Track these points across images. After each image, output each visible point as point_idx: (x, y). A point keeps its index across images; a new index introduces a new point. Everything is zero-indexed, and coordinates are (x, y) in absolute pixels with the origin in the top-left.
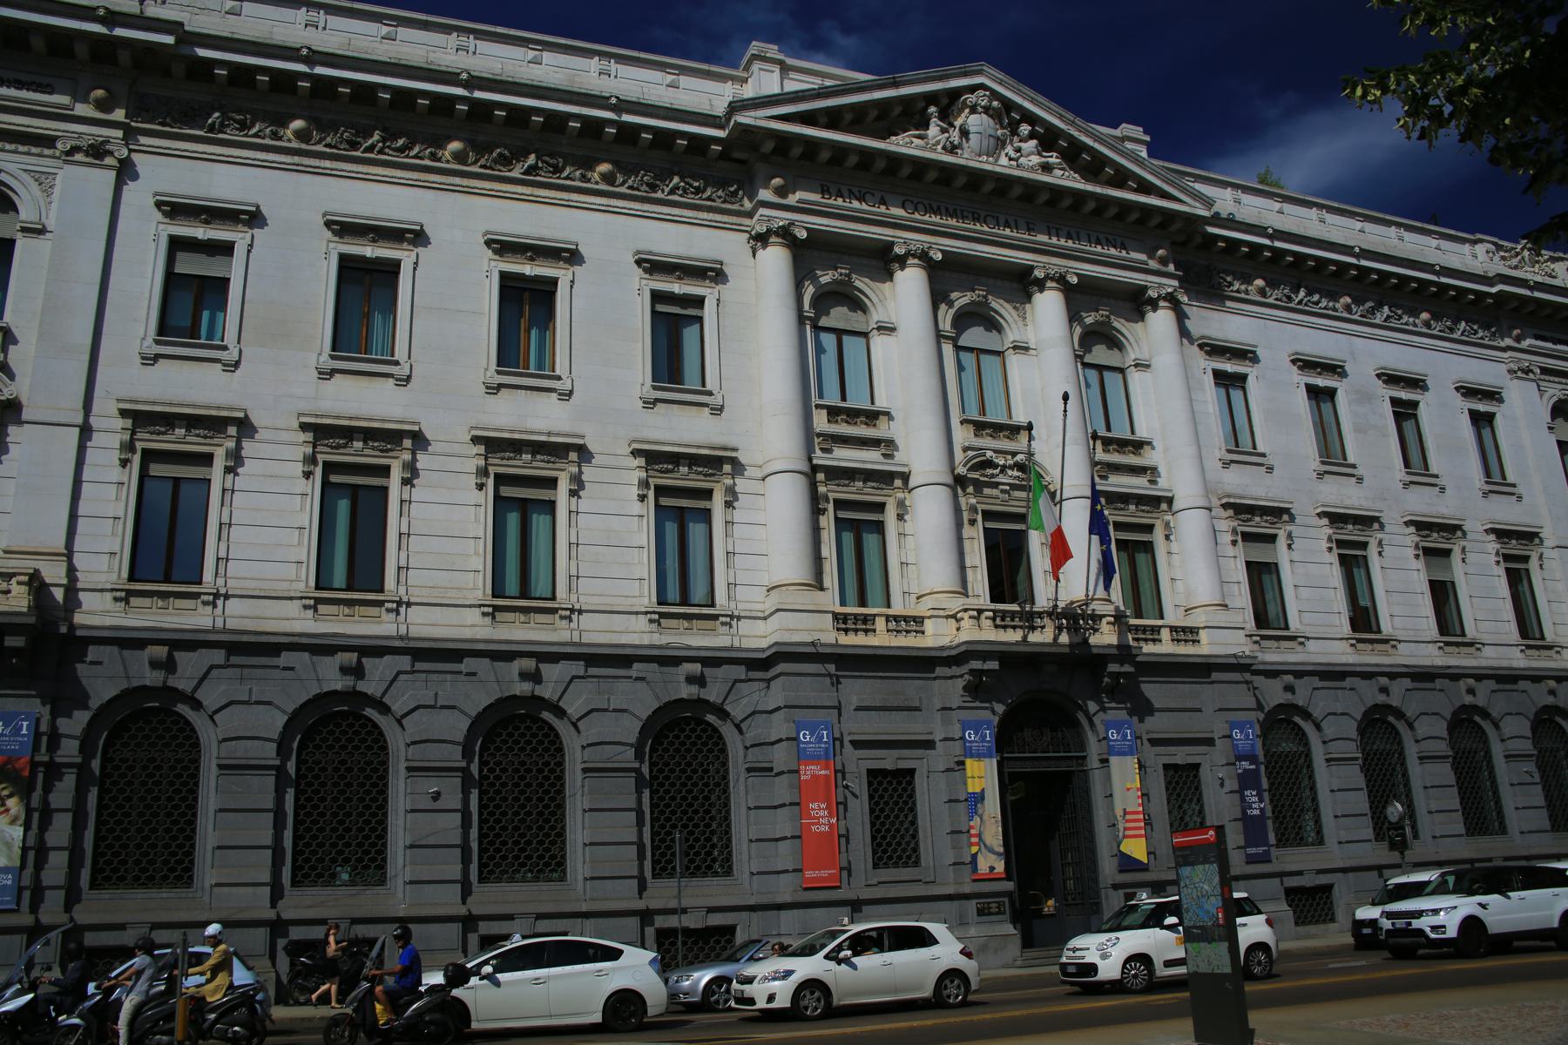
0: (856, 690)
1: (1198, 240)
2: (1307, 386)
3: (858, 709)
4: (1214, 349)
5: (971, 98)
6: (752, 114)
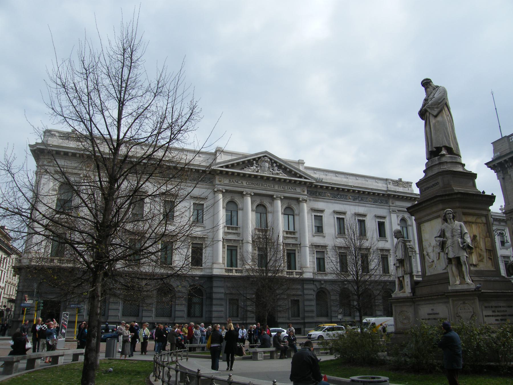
1: (314, 186)
2: (337, 218)
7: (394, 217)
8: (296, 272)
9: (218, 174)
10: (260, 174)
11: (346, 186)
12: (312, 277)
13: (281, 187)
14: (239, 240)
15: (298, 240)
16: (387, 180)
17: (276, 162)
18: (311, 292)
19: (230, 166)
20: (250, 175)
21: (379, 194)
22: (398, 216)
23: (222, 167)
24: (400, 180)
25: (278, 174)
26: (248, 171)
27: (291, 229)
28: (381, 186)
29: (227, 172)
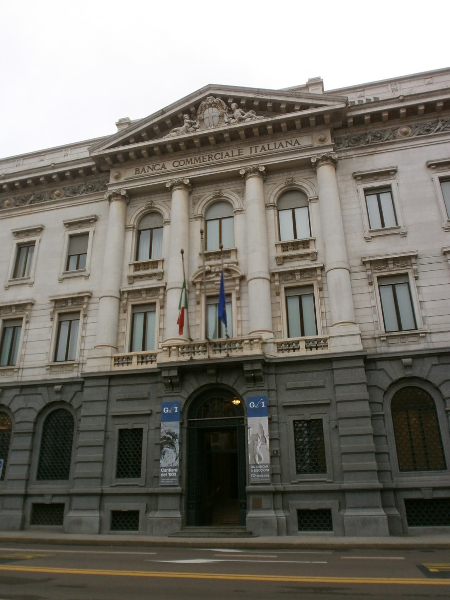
0: (118, 392)
3: (118, 400)
5: (204, 103)
6: (98, 150)
8: (307, 341)
9: (112, 167)
12: (360, 347)
14: (157, 289)
17: (237, 100)
18: (351, 393)
19: (131, 141)
20: (175, 145)
25: (241, 120)
27: (302, 235)
29: (125, 154)
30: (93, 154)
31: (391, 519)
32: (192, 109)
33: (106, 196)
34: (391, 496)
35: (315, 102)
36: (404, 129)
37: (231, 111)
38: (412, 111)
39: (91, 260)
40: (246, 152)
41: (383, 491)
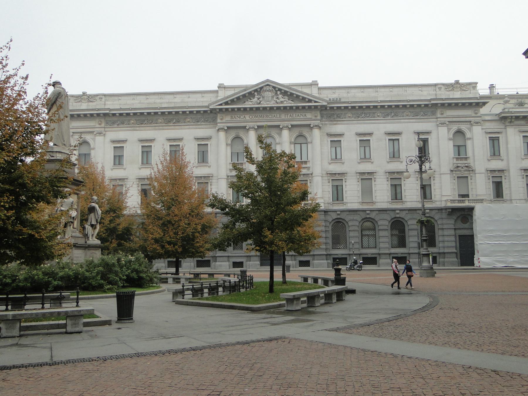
4: (330, 135)
7: (443, 131)
9: (219, 112)
10: (264, 104)
11: (370, 102)
13: (289, 116)
15: (311, 170)
16: (435, 85)
17: (280, 90)
19: (229, 102)
20: (251, 109)
21: (419, 106)
22: (449, 130)
23: (221, 105)
24: (457, 82)
26: (248, 104)
28: (427, 95)
29: (227, 109)
30: (210, 107)
31: (328, 263)
32: (259, 90)
33: (217, 128)
34: (329, 256)
35: (315, 100)
36: (349, 115)
37: (276, 93)
38: (353, 108)
39: (211, 157)
40: (283, 117)
41: (326, 255)
